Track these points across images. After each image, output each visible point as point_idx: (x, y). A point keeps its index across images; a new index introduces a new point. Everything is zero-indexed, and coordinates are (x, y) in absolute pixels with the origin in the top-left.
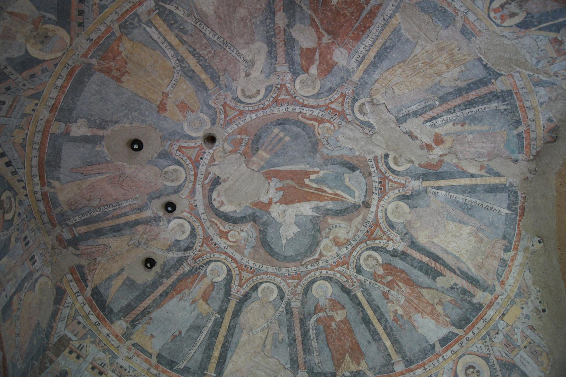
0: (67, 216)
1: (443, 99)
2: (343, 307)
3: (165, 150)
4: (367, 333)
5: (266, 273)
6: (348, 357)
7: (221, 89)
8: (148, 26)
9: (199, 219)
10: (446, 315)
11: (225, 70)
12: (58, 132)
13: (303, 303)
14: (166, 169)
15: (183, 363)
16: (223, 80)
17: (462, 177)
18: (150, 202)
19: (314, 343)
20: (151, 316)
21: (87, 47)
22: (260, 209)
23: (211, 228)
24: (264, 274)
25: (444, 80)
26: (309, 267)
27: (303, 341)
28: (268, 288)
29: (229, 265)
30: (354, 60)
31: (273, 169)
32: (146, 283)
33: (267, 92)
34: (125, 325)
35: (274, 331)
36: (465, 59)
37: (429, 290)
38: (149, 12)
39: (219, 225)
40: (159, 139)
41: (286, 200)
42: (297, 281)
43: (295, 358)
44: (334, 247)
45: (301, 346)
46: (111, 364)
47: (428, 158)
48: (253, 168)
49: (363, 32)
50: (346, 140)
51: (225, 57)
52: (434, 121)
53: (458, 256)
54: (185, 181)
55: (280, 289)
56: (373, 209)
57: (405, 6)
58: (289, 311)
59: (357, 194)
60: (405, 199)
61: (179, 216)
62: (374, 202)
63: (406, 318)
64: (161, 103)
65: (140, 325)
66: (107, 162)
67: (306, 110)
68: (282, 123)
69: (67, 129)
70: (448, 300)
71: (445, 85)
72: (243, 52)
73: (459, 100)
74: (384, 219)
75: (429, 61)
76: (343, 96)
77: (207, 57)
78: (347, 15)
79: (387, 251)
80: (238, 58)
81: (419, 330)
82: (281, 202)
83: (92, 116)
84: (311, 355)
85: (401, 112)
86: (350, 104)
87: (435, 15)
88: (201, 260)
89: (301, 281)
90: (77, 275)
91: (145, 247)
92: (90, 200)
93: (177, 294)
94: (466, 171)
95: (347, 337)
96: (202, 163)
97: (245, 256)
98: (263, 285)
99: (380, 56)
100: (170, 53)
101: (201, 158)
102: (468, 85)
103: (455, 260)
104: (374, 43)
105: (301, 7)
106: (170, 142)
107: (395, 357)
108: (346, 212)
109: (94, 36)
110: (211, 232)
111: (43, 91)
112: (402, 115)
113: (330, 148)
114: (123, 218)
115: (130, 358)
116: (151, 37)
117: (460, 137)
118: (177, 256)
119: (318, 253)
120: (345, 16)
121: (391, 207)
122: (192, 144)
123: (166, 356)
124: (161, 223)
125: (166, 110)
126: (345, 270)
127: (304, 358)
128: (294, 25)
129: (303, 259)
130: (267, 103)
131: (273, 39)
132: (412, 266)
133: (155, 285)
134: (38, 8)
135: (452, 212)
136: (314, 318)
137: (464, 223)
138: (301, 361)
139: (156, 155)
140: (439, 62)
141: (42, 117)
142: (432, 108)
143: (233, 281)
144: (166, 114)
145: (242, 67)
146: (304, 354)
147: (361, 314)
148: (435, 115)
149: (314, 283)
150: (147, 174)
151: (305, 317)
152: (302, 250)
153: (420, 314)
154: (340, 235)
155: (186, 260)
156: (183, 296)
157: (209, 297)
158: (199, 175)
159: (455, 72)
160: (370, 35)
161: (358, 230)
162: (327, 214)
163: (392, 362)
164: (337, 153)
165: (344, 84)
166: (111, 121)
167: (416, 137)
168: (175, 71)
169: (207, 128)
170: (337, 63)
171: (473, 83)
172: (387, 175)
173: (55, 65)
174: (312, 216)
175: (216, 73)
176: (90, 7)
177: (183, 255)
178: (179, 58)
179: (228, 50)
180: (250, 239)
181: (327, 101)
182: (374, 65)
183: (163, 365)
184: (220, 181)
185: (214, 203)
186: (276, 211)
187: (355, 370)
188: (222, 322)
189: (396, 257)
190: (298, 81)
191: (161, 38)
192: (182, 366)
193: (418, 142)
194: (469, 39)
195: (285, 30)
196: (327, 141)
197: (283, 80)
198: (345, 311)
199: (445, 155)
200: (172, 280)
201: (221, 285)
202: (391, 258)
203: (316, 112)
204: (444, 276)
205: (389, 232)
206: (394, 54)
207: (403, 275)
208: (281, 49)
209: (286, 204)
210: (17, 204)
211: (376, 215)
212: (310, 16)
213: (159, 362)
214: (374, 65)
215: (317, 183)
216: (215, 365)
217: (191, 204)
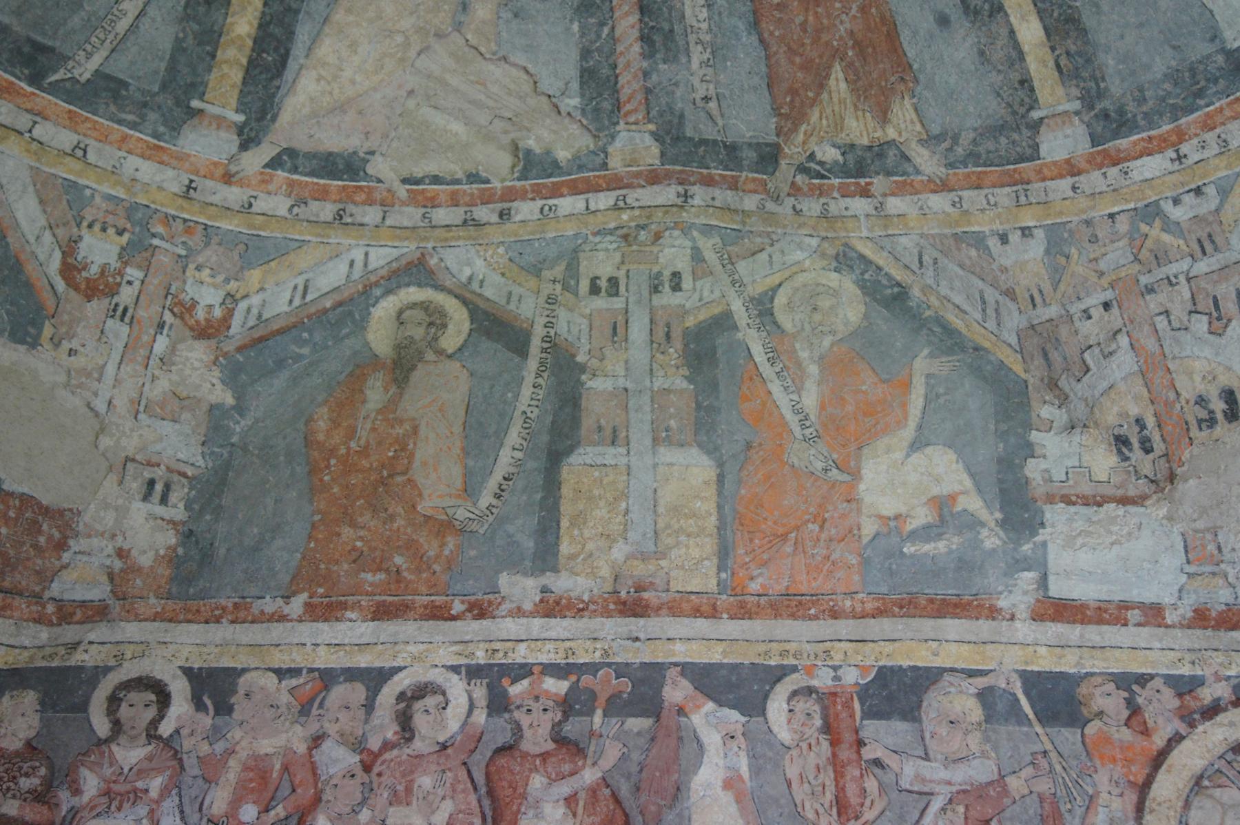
6: (838, 82)
15: (89, 56)
43: (605, 71)
45: (634, 18)
84: (675, 59)
107: (1053, 94)
127: (646, 74)
138: (629, 84)
146: (644, 56)
163: (1036, 115)
187: (865, 142)
192: (85, 69)
216: (237, 76)
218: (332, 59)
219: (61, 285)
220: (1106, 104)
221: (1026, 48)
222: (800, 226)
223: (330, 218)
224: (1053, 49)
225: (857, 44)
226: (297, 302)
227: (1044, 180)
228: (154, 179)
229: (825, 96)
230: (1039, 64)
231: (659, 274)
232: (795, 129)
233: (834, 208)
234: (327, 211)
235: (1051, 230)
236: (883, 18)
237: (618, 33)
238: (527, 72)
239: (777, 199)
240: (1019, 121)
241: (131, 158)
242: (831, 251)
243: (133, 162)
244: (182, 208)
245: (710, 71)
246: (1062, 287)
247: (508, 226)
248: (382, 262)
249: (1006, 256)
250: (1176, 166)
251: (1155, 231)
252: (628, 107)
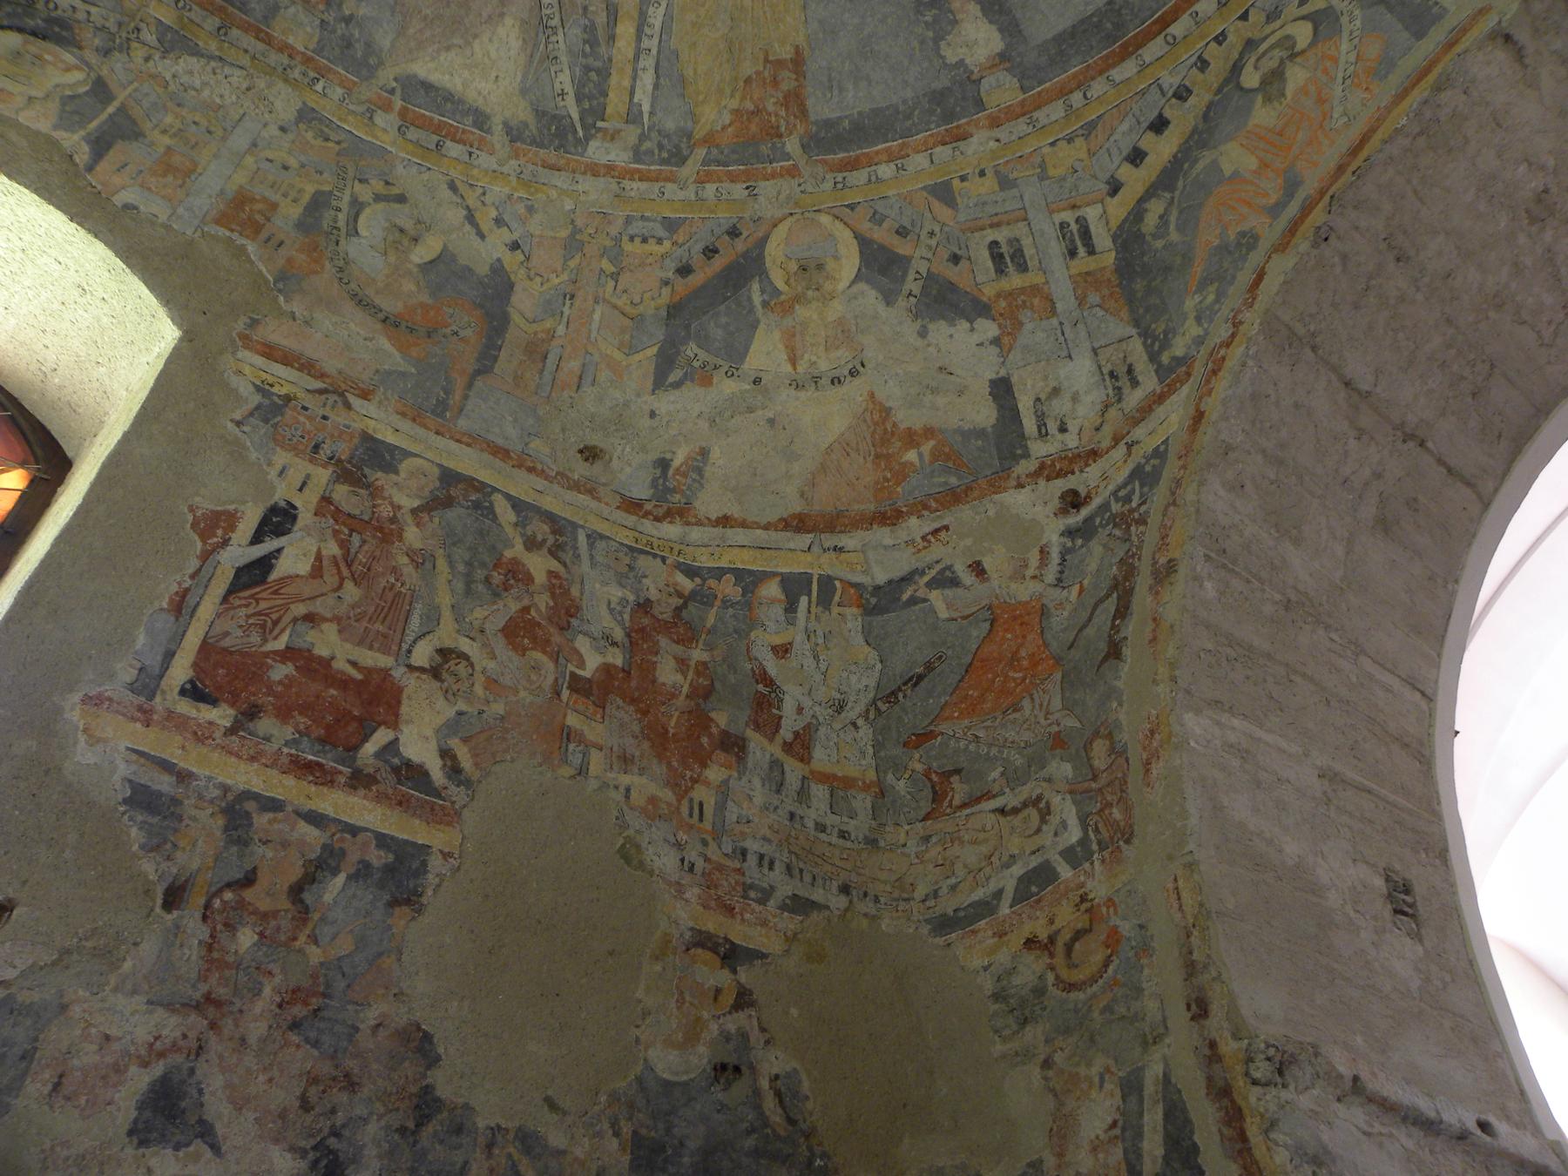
8: (641, 113)
38: (613, 136)
83: (922, 42)
109: (738, 190)
111: (924, 188)
116: (656, 86)
134: (754, 326)
141: (992, 144)
191: (641, 64)
210: (1278, 23)
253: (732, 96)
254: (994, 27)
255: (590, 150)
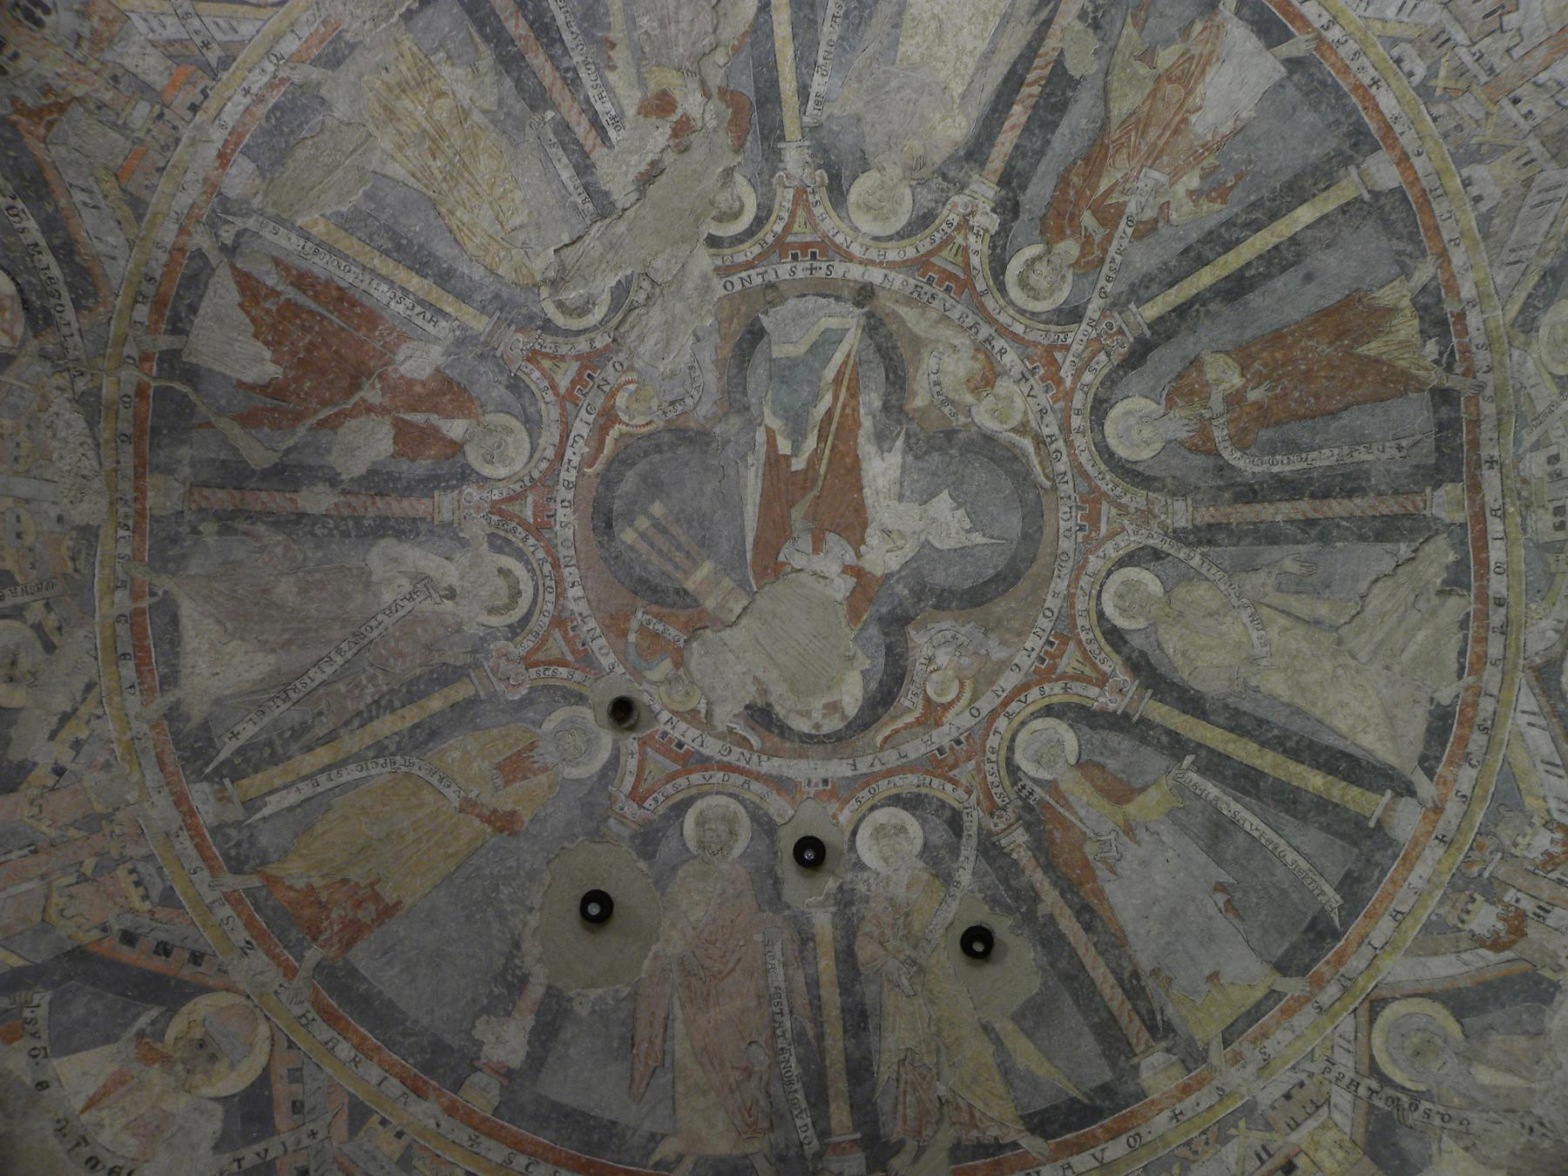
0: (787, 1147)
1: (538, 100)
2: (1195, 362)
3: (633, 837)
4: (1279, 284)
5: (1070, 598)
6: (1372, 348)
7: (477, 666)
8: (259, 809)
9: (868, 780)
10: (1185, 32)
11: (429, 648)
12: (494, 1097)
13: (1181, 490)
14: (691, 844)
15: (1323, 893)
16: (455, 656)
17: (770, 35)
18: (788, 907)
19: (1323, 459)
20: (1149, 969)
21: (267, 959)
22: (870, 601)
23: (904, 748)
24: (1072, 606)
25: (480, 102)
26: (1060, 467)
27: (1313, 496)
28: (1121, 596)
29: (1031, 709)
30: (429, 327)
31: (749, 556)
32: (1040, 967)
33: (507, 550)
34: (1158, 1057)
35: (1269, 589)
36: (413, 54)
37: (1113, 95)
38: (223, 798)
39: (899, 724)
40: (597, 847)
41: (854, 524)
42: (1105, 506)
43: (1378, 524)
44: (997, 390)
45: (1334, 503)
46: (1269, 1127)
47: (715, 130)
48: (738, 609)
49: (354, 304)
50: (673, 355)
51: (392, 644)
52: (604, 119)
53: (998, 20)
54: (742, 802)
55: (1128, 560)
56: (876, 276)
57: (275, 204)
58: (1204, 536)
59: (833, 323)
60: (840, 186)
61: (847, 834)
62: (855, 272)
63: (1210, 161)
64: (489, 822)
65: (1170, 1011)
66: (634, 996)
67: (573, 455)
68: (604, 521)
69: (497, 1072)
70: (1135, 34)
71: (493, 99)
72: (388, 598)
73: (538, 60)
74: (904, 242)
75: (428, 143)
76: (533, 357)
77: (385, 688)
78: (311, 343)
79: (1004, 230)
80: (401, 613)
81: (1244, 115)
82: (858, 542)
83: (474, 1000)
85: (580, 206)
86: (560, 340)
87: (292, 131)
88: (1000, 790)
89: (1105, 494)
90: (977, 1167)
91: (928, 949)
92: (748, 1073)
93: (1095, 879)
94: (752, 25)
95: (1297, 353)
96: (696, 745)
97: (1012, 656)
98: (1109, 610)
99: (420, 261)
100: (350, 774)
101: (680, 745)
102: (487, 39)
103: (1011, 25)
104: (384, 278)
105: (289, 451)
106: (612, 821)
107: (1348, 188)
108: (890, 355)
109: (241, 936)
110: (915, 749)
111: (351, 1095)
112: (590, 205)
113: (697, 396)
114: (822, 992)
115: (1267, 1061)
116: (291, 809)
117: (647, 49)
118: (972, 859)
119: (1016, 438)
120: (312, 347)
121: (869, 222)
122: (632, 764)
123: (1286, 945)
124: (862, 888)
125: (513, 813)
126: (1070, 358)
128: (331, 468)
129: (1035, 485)
130: (541, 554)
131: (366, 523)
132: (1041, 153)
133: (1050, 940)
135: (870, 50)
136: (1231, 456)
137: (900, 14)
138: (1390, 506)
139: (642, 865)
140: (429, 115)
142: (564, 128)
143: (1085, 702)
144: (526, 815)
145: (428, 605)
147: (1213, 306)
148: (584, 120)
149: (1112, 455)
150: (697, 898)
151: (1228, 486)
152: (1007, 485)
153: (1193, 118)
154: (962, 373)
155: (990, 834)
156: (1104, 861)
157: (1121, 781)
158: (732, 758)
159: (454, 77)
160: (363, 286)
161: (944, 318)
162: (901, 410)
163: (1367, 197)
164: (710, 378)
165: (498, 353)
166: (510, 957)
167: (653, 164)
168: (404, 769)
169: (591, 717)
170: (438, 370)
171: (481, 31)
172: (770, 239)
173: (290, 1047)
174: (905, 452)
175: (432, 672)
176: (155, 924)
177: (974, 842)
178: (371, 754)
179: (374, 634)
180: (961, 639)
181: (550, 397)
182: (445, 278)
183: (1315, 961)
184: (760, 703)
185: (825, 730)
186: (881, 558)
187: (1416, 322)
188: (1211, 751)
189: (1017, 203)
190: (487, 471)
191: (300, 786)
192: (1332, 898)
193: (670, 157)
194: (352, 47)
195: (345, 493)
196: (672, 403)
197: (478, 509)
198: (1208, 357)
199: (703, 83)
200: (1047, 886)
201: (1088, 741)
202: (1024, 216)
203: (581, 428)
204: (1062, 53)
205: (944, 226)
206: (414, 226)
207: (1075, 179)
208: (395, 505)
209: (864, 526)
211: (892, 265)
212: (310, 429)
213: (1303, 971)
214: (445, 278)
215: (805, 436)
216: (1355, 791)
217: (817, 794)
218: (1350, 721)
219: (1508, 954)
220: (1346, 147)
221: (1318, 215)
222: (1502, 364)
223: (1486, 737)
224: (1314, 195)
225: (1339, 337)
226: (1561, 772)
227: (1418, 179)
228: (1429, 866)
229: (1384, 357)
230: (1328, 203)
231: (1550, 475)
232: (1416, 378)
233: (1480, 340)
234: (1478, 740)
235: (1459, 163)
236: (1316, 321)
237: (1345, 514)
238: (1376, 580)
239: (1481, 387)
240: (1376, 209)
241: (1410, 879)
242: (1522, 337)
243: (1413, 879)
244: (1459, 849)
245: (1374, 446)
246: (1508, 142)
247: (1511, 601)
248: (1533, 700)
249: (1492, 194)
250: (1382, 83)
251: (1440, 83)
252: (1410, 508)
253: (323, 876)
254: (527, 1048)
255: (198, 786)
